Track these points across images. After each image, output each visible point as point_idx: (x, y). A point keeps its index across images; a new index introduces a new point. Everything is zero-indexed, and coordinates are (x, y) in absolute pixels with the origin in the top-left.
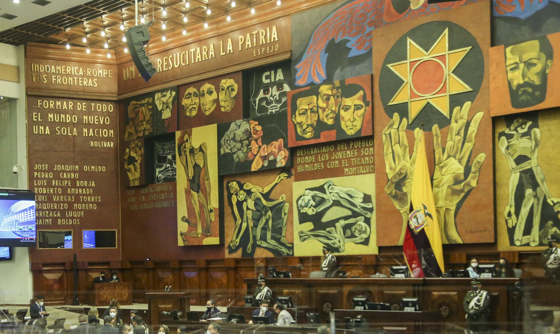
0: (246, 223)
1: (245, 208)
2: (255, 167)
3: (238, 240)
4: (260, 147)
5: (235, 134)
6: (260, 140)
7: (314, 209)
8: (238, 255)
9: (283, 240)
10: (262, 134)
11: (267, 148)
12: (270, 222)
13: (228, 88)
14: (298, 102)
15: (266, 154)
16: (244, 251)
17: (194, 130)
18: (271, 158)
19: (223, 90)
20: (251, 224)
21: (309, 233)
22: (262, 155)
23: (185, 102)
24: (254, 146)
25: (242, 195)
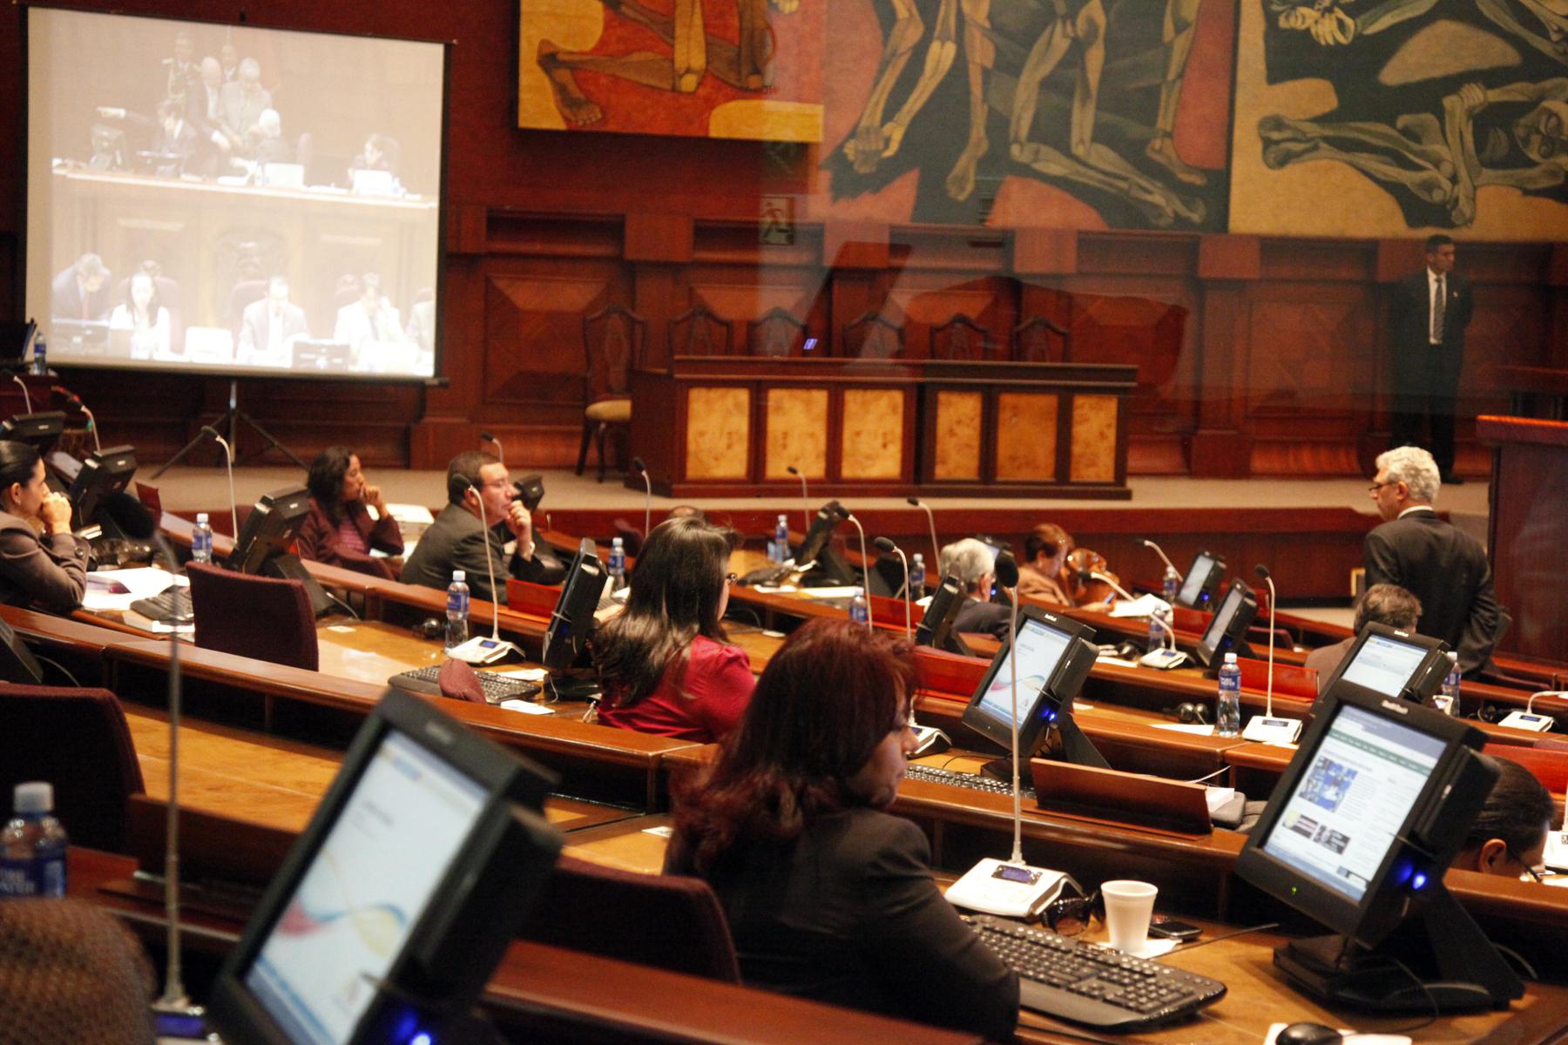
0: (950, 49)
3: (896, 132)
7: (1349, 22)
8: (895, 206)
9: (1161, 150)
12: (1095, 58)
16: (931, 191)
20: (982, 53)
21: (1314, 130)
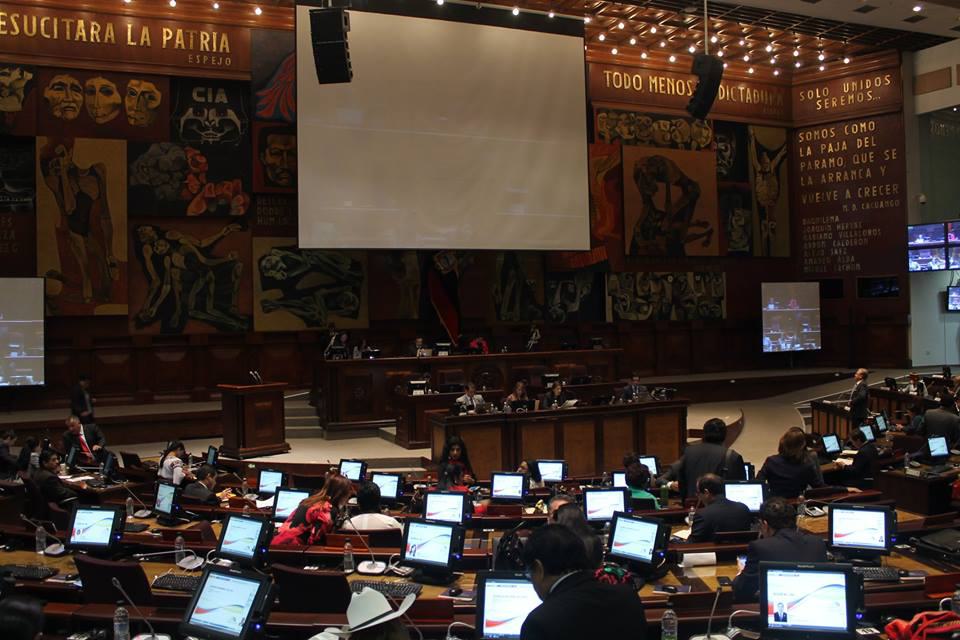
0: (169, 287)
1: (167, 264)
2: (192, 211)
3: (154, 310)
4: (202, 185)
5: (158, 161)
6: (204, 175)
7: (285, 274)
8: (156, 328)
10: (207, 168)
11: (215, 189)
12: (212, 287)
13: (143, 93)
14: (270, 138)
15: (214, 196)
17: (77, 140)
18: (222, 202)
19: (133, 94)
20: (178, 287)
22: (206, 195)
23: (49, 94)
24: (193, 184)
25: (162, 247)
